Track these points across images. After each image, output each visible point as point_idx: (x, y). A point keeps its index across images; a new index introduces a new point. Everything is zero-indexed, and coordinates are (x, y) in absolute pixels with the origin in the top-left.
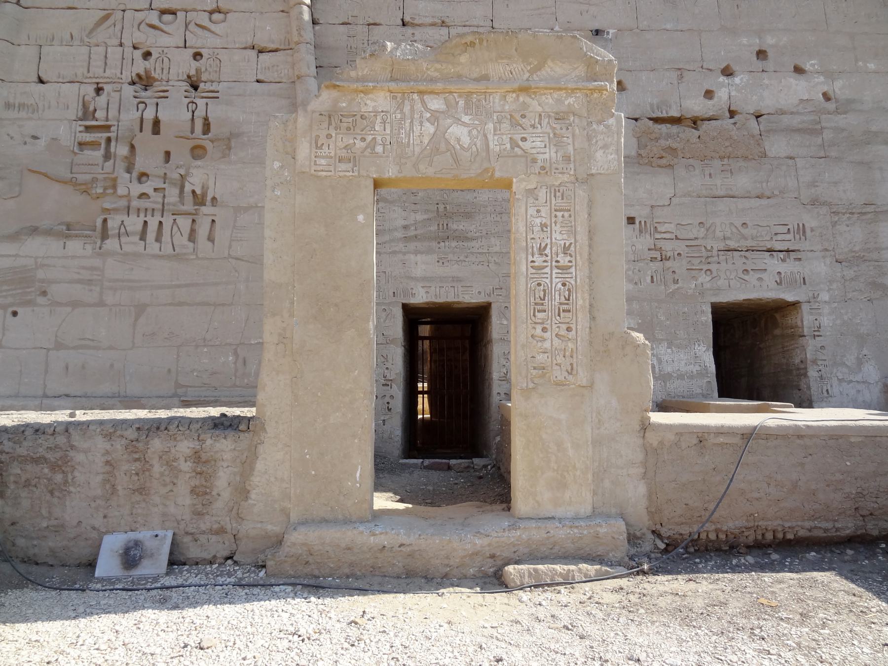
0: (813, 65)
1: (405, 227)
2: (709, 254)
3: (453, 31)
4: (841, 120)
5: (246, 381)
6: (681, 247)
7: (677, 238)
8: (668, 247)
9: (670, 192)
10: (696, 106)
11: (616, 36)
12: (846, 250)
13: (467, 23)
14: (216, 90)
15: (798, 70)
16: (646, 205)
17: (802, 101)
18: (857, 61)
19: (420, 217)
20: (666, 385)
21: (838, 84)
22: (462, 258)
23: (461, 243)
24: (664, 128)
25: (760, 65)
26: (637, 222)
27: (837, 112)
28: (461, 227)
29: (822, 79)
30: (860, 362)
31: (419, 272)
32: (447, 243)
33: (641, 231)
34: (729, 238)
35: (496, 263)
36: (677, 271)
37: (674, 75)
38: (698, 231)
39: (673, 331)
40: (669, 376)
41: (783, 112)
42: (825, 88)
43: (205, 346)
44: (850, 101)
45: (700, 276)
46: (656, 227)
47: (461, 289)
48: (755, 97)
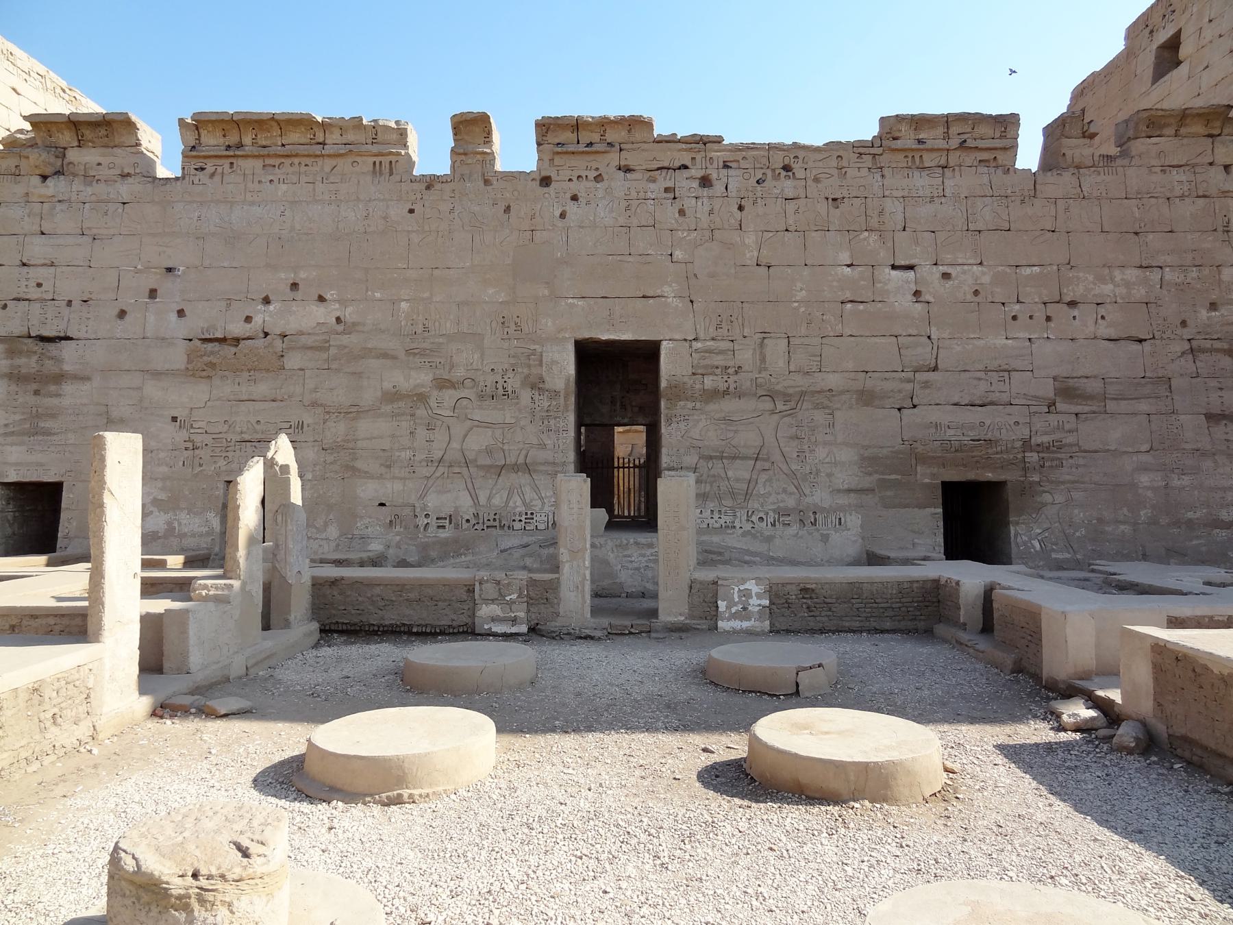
0: (332, 295)
1: (6, 425)
2: (229, 444)
3: (59, 270)
4: (345, 340)
6: (208, 439)
8: (198, 439)
9: (206, 397)
10: (237, 328)
11: (184, 272)
12: (331, 441)
15: (321, 299)
17: (318, 324)
18: (367, 291)
20: (181, 542)
21: (349, 310)
24: (210, 346)
25: (291, 295)
27: (344, 333)
28: (47, 425)
29: (337, 306)
30: (326, 525)
31: (13, 458)
33: (180, 427)
34: (245, 433)
37: (223, 304)
40: (185, 535)
41: (301, 333)
42: (338, 314)
44: (354, 324)
48: (283, 322)
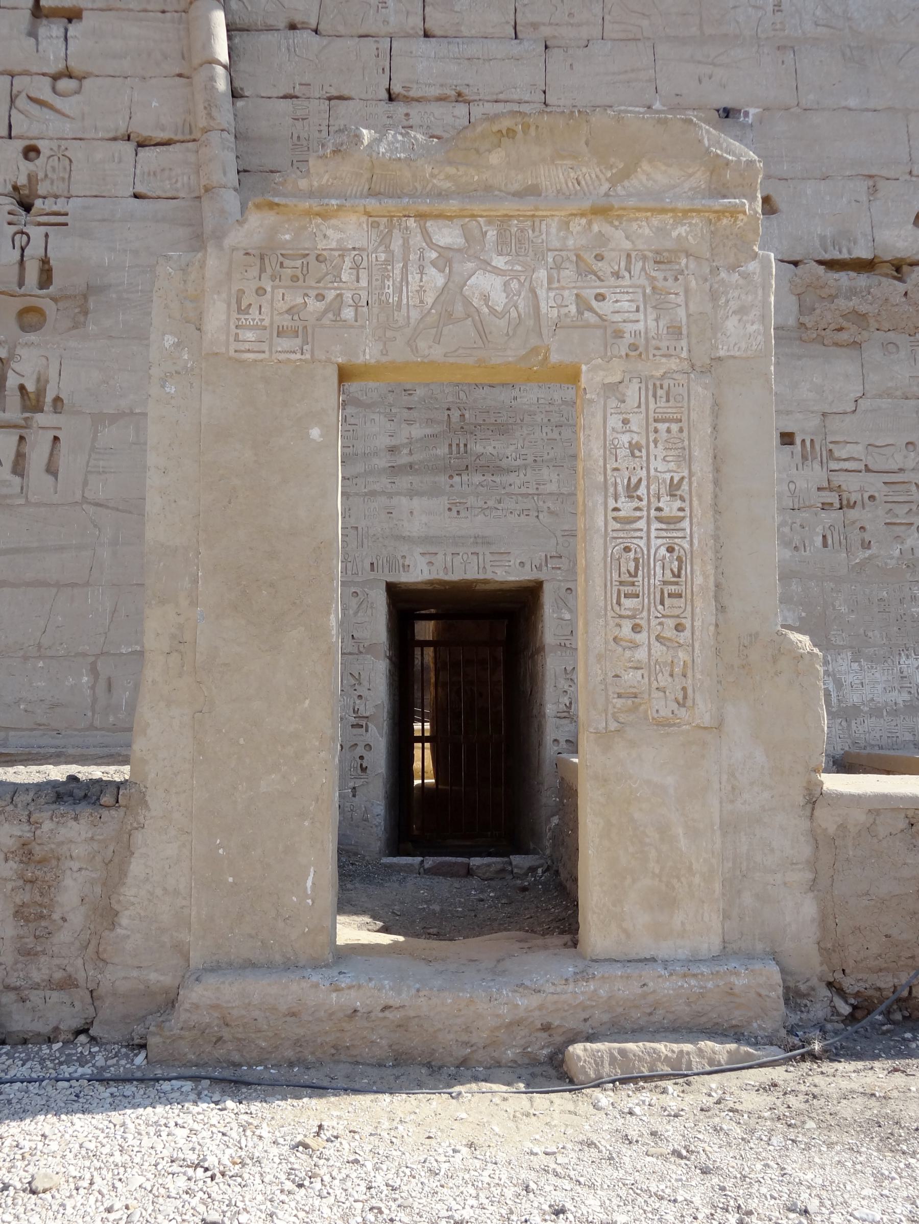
1: (392, 450)
3: (478, 111)
5: (111, 719)
6: (874, 484)
7: (868, 469)
8: (852, 484)
9: (855, 390)
11: (760, 120)
13: (501, 97)
14: (63, 211)
16: (812, 412)
19: (417, 431)
20: (849, 726)
22: (491, 503)
23: (489, 478)
24: (844, 278)
26: (798, 441)
28: (490, 449)
31: (415, 527)
32: (465, 478)
33: (804, 457)
35: (551, 513)
36: (868, 527)
37: (862, 186)
38: (905, 457)
39: (862, 631)
43: (40, 657)
45: (909, 536)
46: (831, 450)
47: (489, 557)
